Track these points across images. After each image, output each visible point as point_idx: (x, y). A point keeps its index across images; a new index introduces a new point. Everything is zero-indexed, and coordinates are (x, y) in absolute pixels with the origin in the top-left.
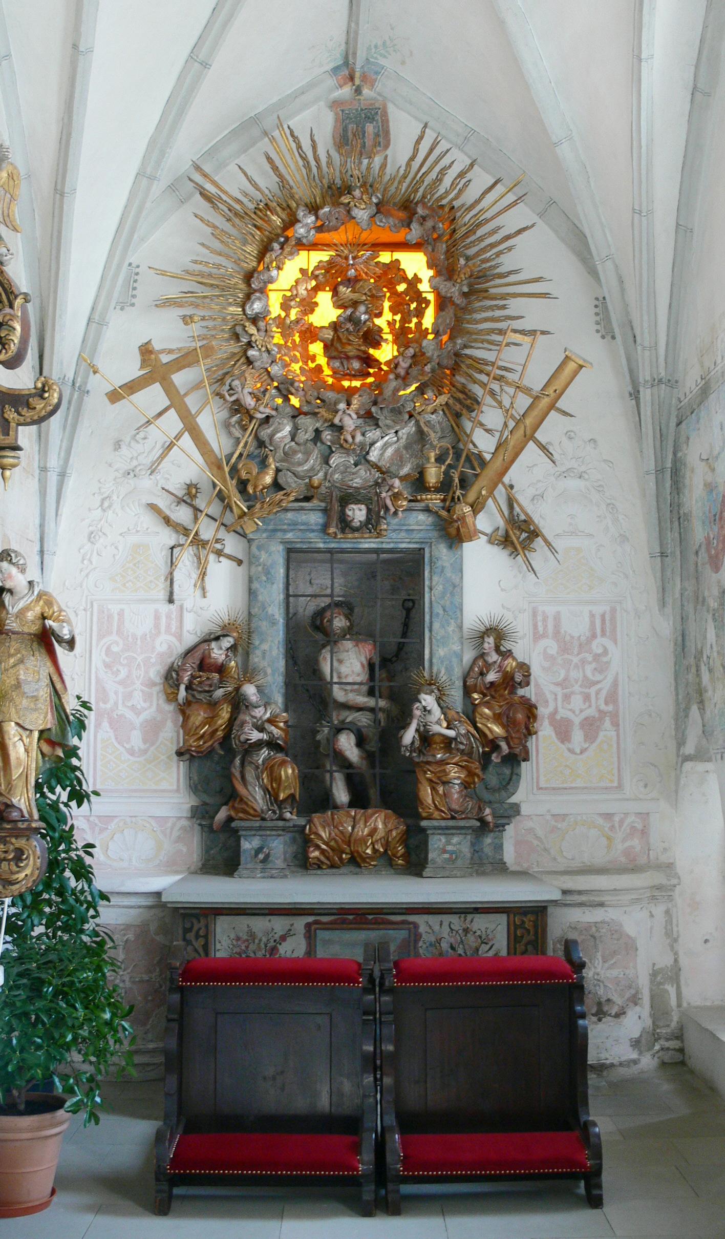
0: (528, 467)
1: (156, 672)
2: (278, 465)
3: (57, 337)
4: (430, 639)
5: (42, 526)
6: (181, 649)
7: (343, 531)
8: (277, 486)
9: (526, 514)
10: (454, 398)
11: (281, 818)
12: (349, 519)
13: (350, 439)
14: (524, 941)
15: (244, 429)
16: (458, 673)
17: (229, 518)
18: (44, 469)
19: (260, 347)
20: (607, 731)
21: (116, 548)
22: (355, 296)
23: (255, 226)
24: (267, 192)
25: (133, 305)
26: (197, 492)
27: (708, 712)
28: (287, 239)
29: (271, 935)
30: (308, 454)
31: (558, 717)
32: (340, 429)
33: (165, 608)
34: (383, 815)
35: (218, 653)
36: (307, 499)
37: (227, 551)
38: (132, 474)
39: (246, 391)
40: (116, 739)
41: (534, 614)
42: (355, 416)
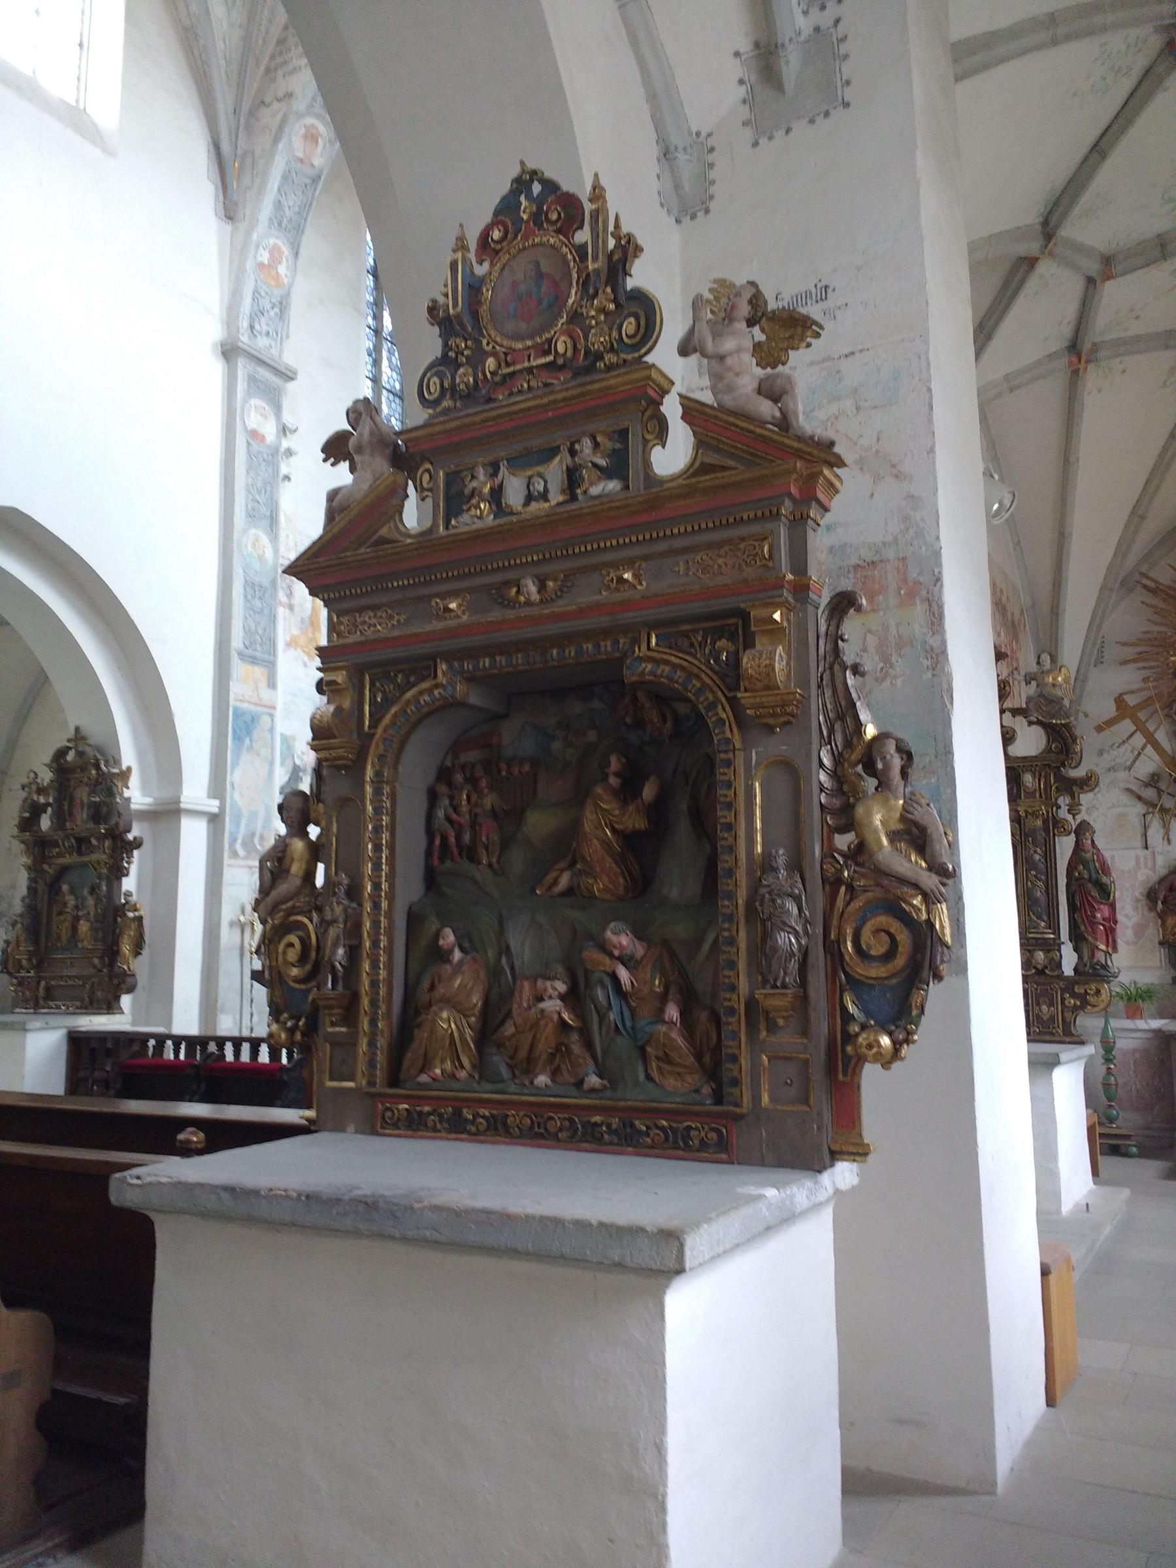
6: (1155, 878)
25: (1102, 662)
33: (1142, 853)
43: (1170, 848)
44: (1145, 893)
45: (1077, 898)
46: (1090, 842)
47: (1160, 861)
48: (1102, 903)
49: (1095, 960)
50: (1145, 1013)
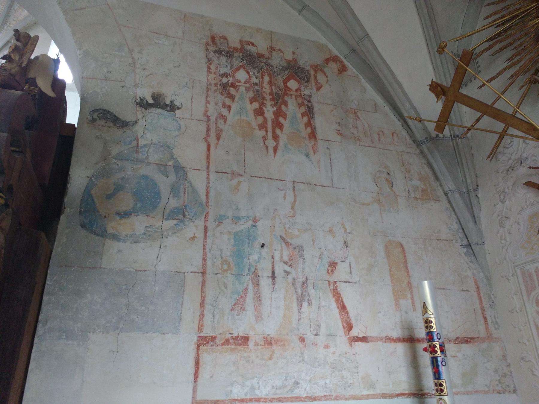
21: (519, 224)
38: (510, 170)
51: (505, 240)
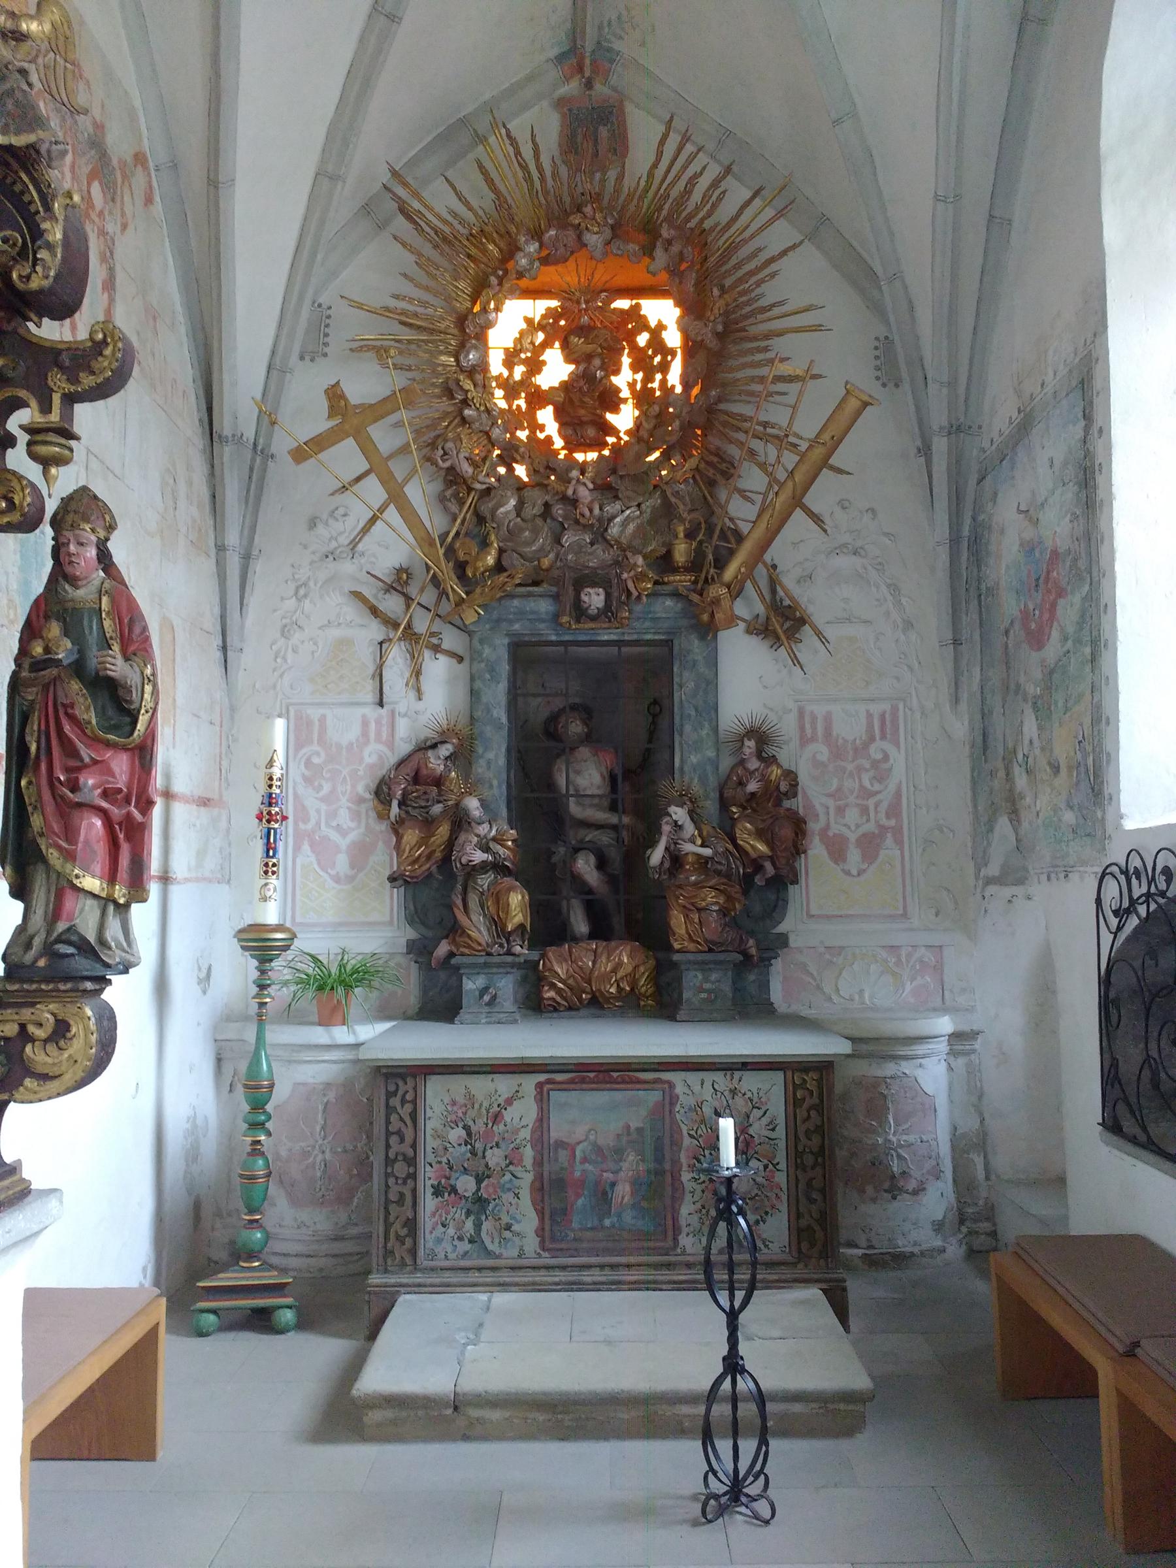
0: (793, 543)
1: (363, 787)
2: (501, 544)
3: (226, 377)
4: (681, 743)
5: (223, 617)
6: (393, 760)
7: (578, 621)
8: (499, 568)
9: (792, 598)
10: (707, 463)
11: (509, 953)
12: (585, 606)
13: (587, 513)
14: (805, 1106)
15: (461, 503)
16: (713, 781)
17: (446, 607)
18: (221, 548)
19: (478, 406)
20: (889, 851)
21: (315, 644)
22: (590, 348)
23: (469, 256)
24: (480, 212)
25: (325, 355)
26: (408, 577)
27: (1025, 825)
28: (506, 272)
29: (493, 1098)
30: (536, 532)
31: (831, 834)
32: (574, 502)
33: (372, 712)
34: (628, 948)
35: (436, 762)
36: (536, 583)
37: (445, 646)
38: (331, 558)
39: (461, 456)
40: (319, 864)
41: (801, 713)
42: (591, 486)
43: (420, 706)
44: (373, 786)
45: (34, 725)
46: (92, 552)
47: (403, 728)
48: (109, 745)
49: (61, 926)
50: (354, 1010)
51: (285, 659)
